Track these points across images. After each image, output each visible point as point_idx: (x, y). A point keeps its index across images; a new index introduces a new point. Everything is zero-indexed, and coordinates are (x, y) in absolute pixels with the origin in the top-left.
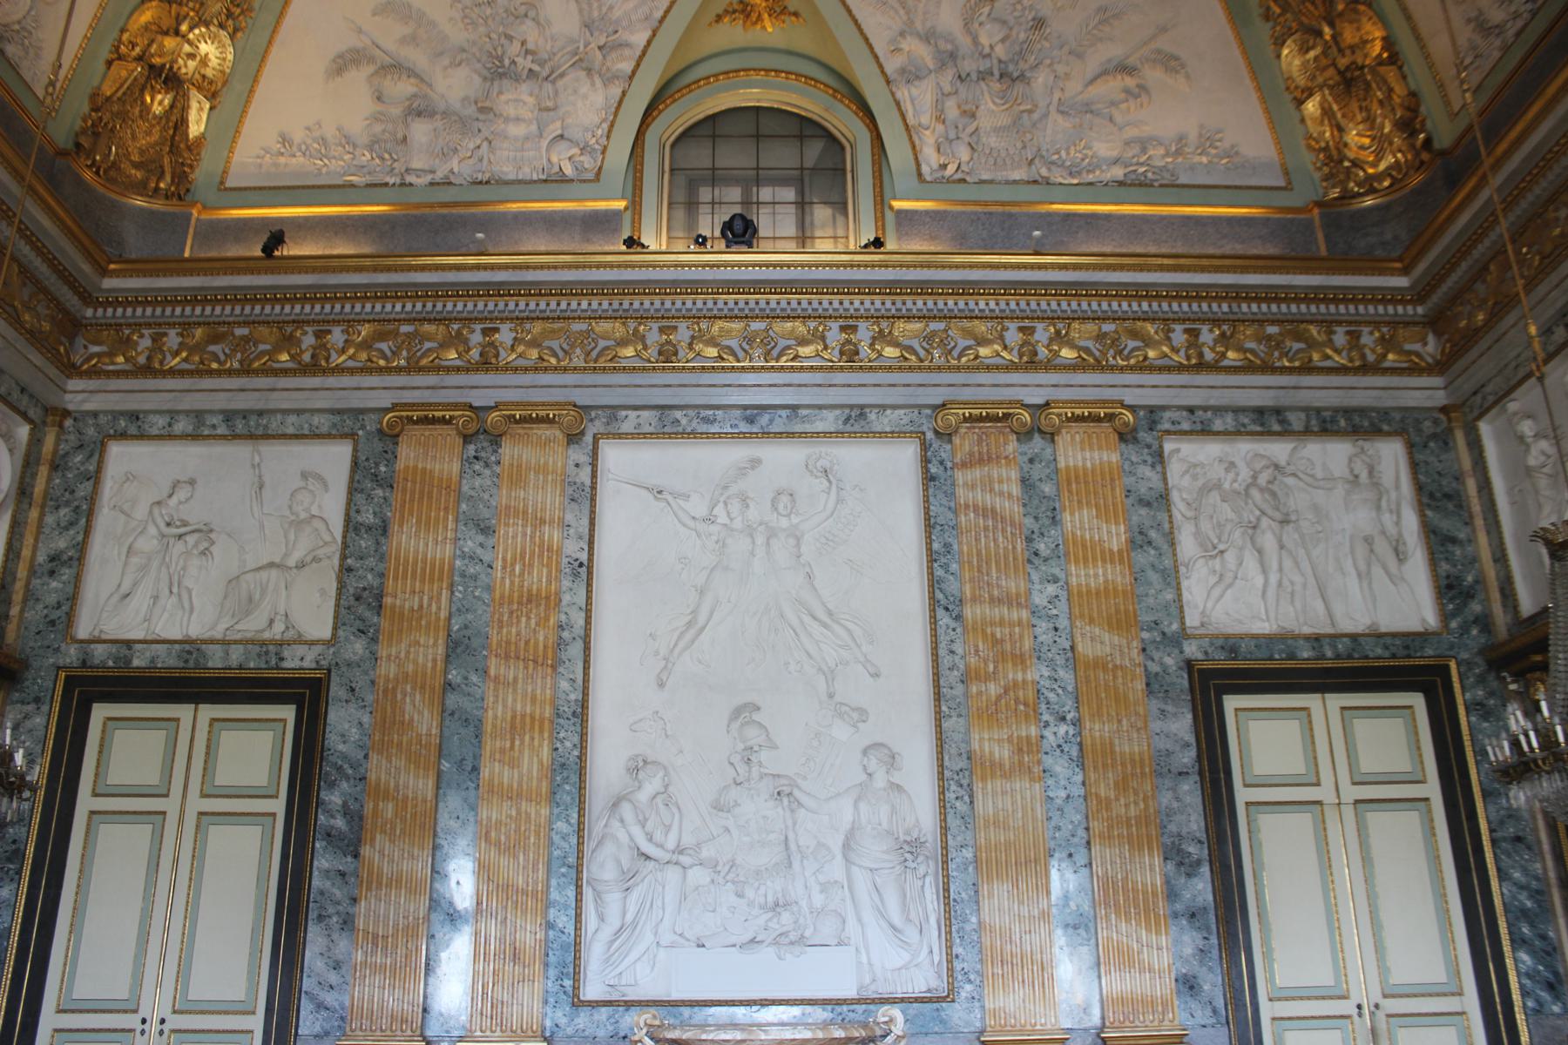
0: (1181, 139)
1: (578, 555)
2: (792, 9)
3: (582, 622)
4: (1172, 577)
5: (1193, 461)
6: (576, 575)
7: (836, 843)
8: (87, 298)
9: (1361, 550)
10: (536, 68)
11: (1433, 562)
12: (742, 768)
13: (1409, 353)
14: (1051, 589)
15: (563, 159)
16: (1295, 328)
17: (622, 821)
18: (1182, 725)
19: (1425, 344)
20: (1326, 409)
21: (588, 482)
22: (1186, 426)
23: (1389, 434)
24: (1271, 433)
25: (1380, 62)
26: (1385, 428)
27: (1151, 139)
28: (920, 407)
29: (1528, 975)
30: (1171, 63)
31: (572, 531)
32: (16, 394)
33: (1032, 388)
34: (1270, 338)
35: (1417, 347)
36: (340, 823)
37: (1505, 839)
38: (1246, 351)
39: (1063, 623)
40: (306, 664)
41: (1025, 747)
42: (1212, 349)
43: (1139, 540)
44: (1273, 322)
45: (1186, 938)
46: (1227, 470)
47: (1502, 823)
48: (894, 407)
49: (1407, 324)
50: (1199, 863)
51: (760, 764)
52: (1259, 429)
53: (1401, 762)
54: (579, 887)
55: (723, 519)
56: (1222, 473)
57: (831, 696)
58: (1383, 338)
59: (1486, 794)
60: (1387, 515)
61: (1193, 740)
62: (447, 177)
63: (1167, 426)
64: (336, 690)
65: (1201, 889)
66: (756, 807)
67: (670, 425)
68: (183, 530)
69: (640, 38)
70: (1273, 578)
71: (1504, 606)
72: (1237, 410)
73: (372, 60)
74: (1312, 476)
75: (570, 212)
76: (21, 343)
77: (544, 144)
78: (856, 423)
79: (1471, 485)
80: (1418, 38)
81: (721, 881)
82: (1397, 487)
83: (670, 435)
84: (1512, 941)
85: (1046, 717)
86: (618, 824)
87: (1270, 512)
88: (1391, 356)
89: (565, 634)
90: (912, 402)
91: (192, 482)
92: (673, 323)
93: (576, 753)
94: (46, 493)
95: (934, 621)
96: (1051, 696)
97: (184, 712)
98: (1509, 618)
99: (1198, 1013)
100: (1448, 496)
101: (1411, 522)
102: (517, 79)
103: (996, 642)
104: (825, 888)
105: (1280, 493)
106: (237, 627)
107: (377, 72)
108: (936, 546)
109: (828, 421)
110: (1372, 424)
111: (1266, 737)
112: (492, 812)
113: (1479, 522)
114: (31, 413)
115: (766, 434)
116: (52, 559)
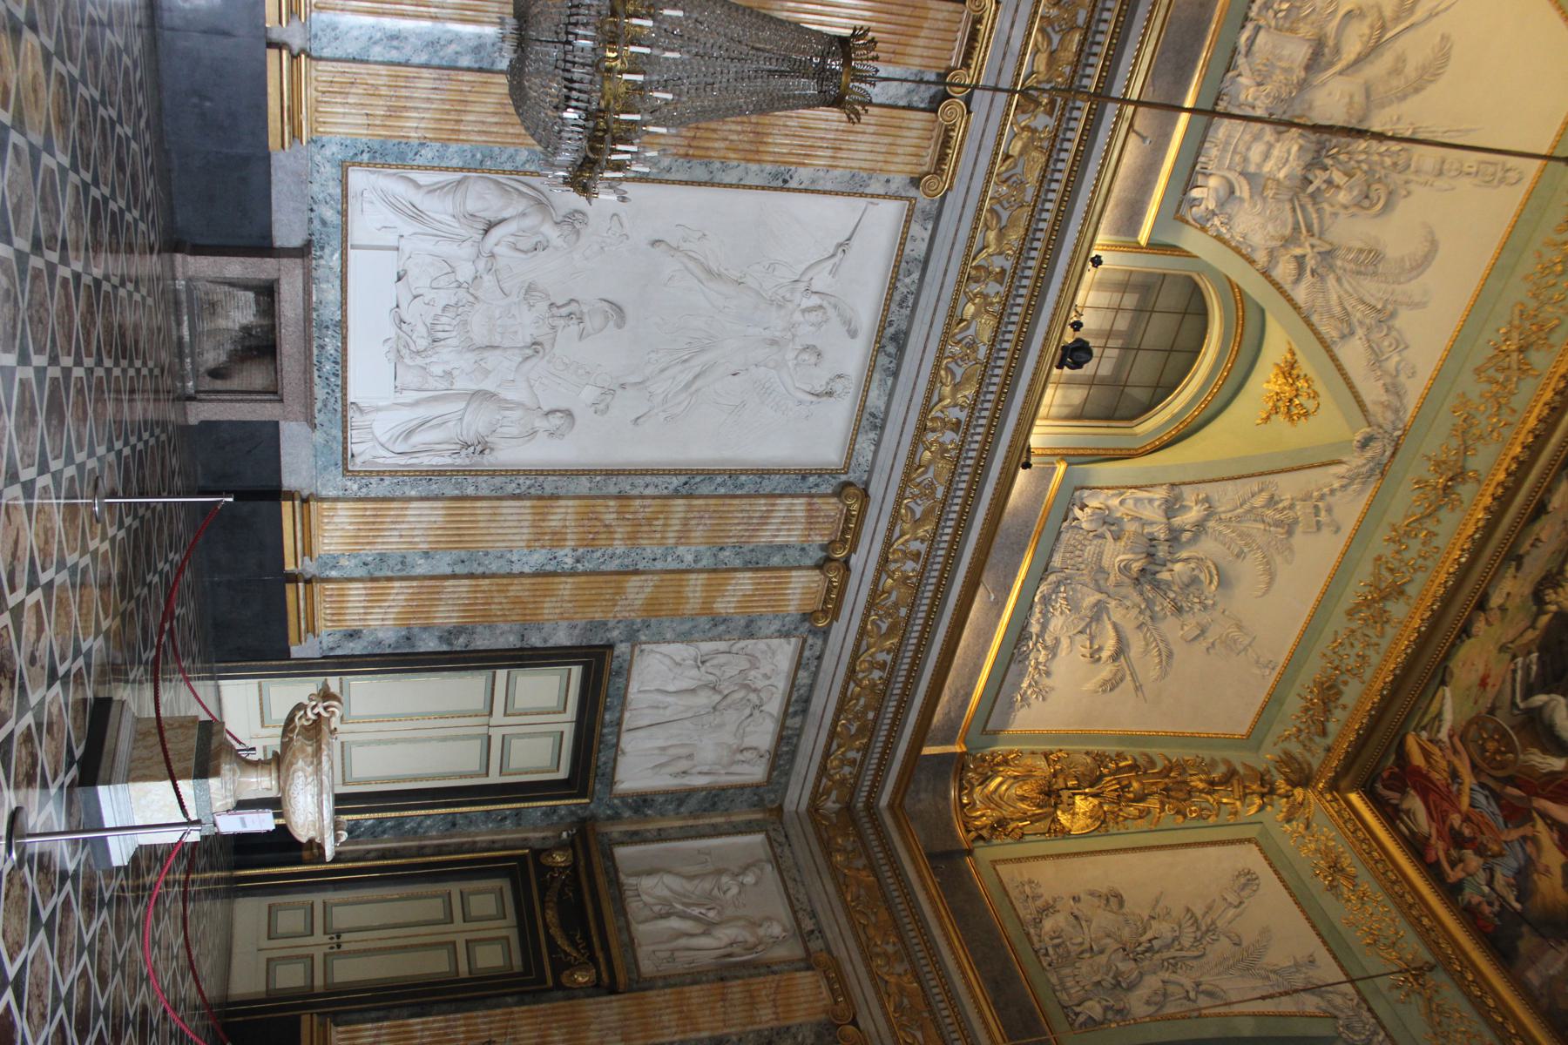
0: (1048, 674)
1: (796, 178)
2: (1273, 417)
3: (727, 180)
4: (685, 637)
5: (780, 656)
6: (776, 176)
7: (488, 385)
10: (1311, 189)
11: (666, 793)
12: (564, 311)
14: (689, 558)
15: (1206, 193)
16: (869, 730)
17: (524, 215)
18: (562, 638)
21: (868, 191)
22: (807, 653)
25: (1055, 820)
27: (1054, 655)
28: (870, 472)
30: (1112, 684)
31: (821, 174)
33: (864, 560)
34: (865, 713)
35: (834, 796)
39: (659, 565)
41: (558, 538)
43: (717, 620)
44: (875, 720)
45: (391, 633)
48: (875, 453)
49: (852, 794)
50: (450, 644)
54: (461, 169)
55: (806, 303)
56: (762, 671)
57: (623, 386)
61: (551, 643)
62: (1236, 67)
63: (810, 641)
65: (430, 644)
66: (527, 323)
67: (907, 269)
69: (1301, 294)
71: (626, 832)
72: (812, 687)
73: (1397, 19)
75: (1163, 158)
77: (1232, 176)
78: (869, 421)
80: (1059, 856)
83: (897, 266)
85: (581, 550)
86: (521, 209)
89: (717, 165)
90: (877, 470)
92: (1057, 112)
95: (677, 473)
96: (599, 554)
98: (615, 835)
99: (331, 639)
100: (714, 804)
102: (1309, 167)
103: (649, 521)
104: (448, 374)
107: (1381, 17)
108: (743, 478)
109: (876, 399)
111: (546, 692)
115: (879, 347)
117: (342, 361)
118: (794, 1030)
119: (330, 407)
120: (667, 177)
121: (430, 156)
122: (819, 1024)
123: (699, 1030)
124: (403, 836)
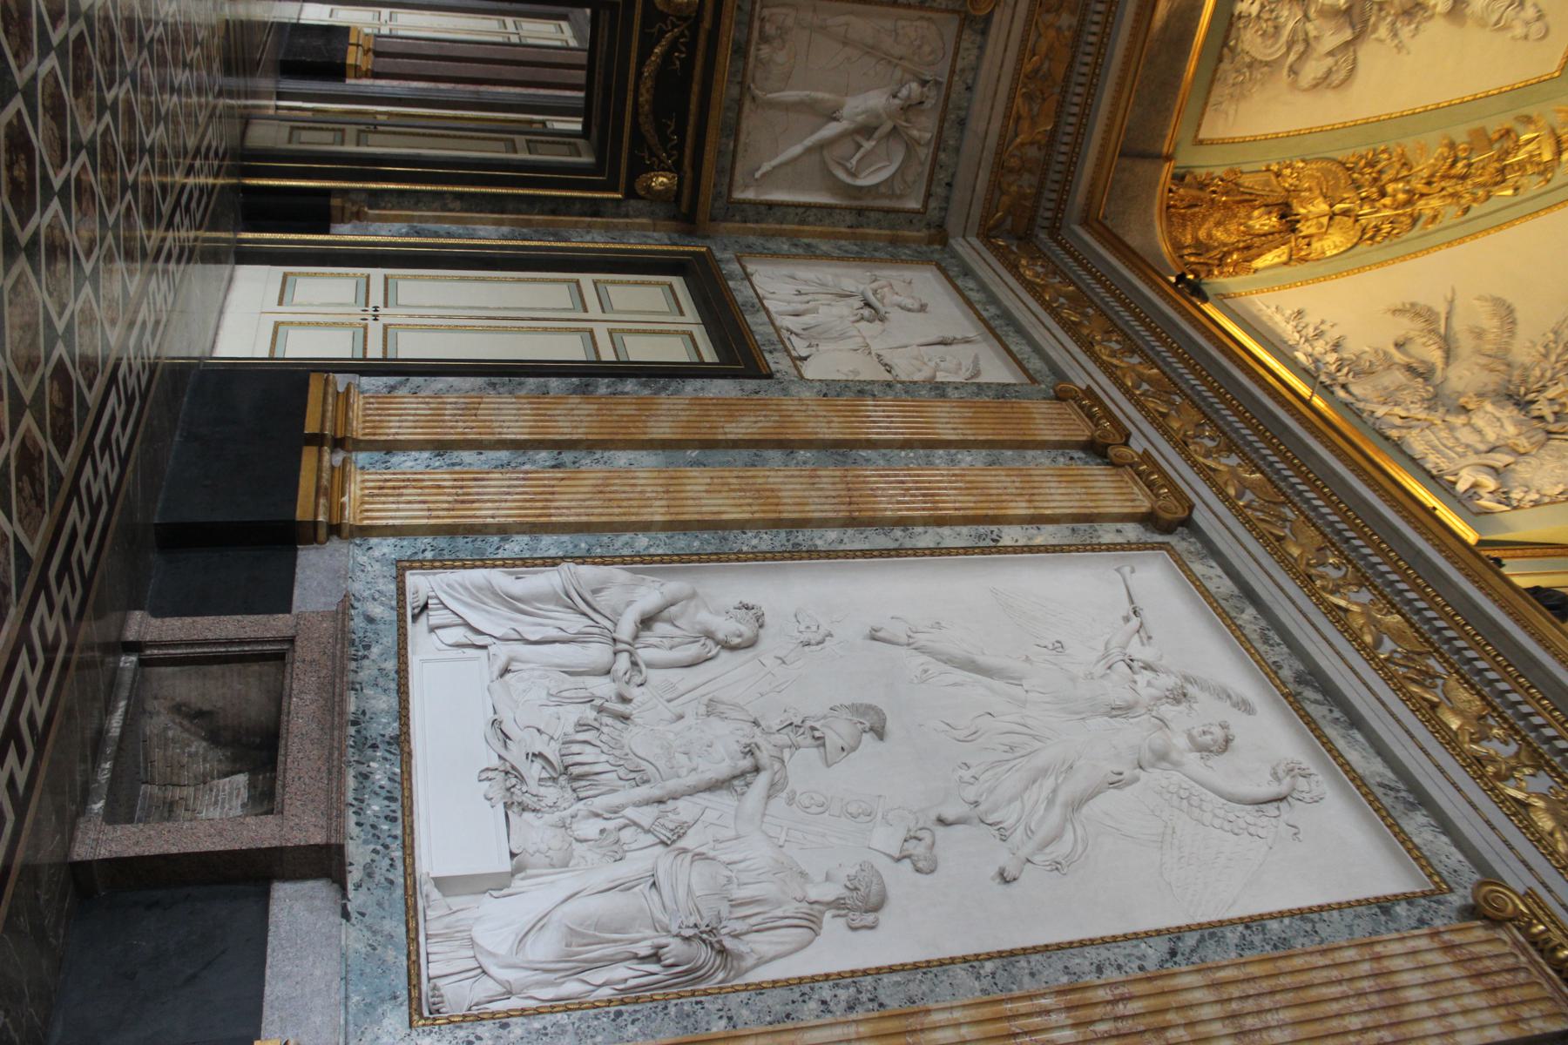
3: (921, 545)
8: (1054, 230)
32: (942, 176)
36: (603, 390)
40: (773, 367)
51: (795, 747)
64: (750, 384)
67: (1236, 608)
68: (873, 300)
76: (988, 156)
81: (597, 702)
91: (923, 308)
93: (745, 549)
94: (865, 237)
97: (691, 313)
106: (793, 338)
112: (643, 478)
114: (933, 204)
115: (1294, 700)
116: (809, 246)
117: (402, 796)
119: (377, 877)
120: (842, 547)
121: (517, 549)
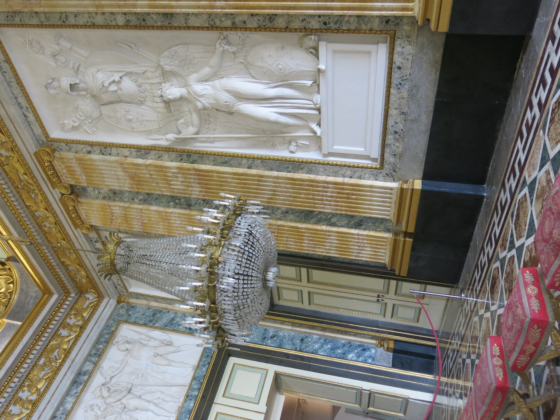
9: (159, 360)
13: (88, 307)
16: (45, 350)
19: (89, 298)
20: (91, 351)
23: (116, 329)
24: (87, 382)
26: (113, 329)
29: (358, 357)
34: (44, 364)
35: (88, 302)
37: (301, 346)
38: (42, 378)
42: (32, 394)
46: (92, 410)
47: (294, 344)
52: (81, 387)
53: (256, 377)
56: (93, 413)
58: (75, 314)
59: (280, 347)
60: (150, 342)
70: (152, 407)
72: (67, 393)
74: (117, 369)
79: (154, 304)
82: (141, 334)
84: (342, 359)
87: (120, 397)
88: (85, 315)
100: (154, 315)
101: (157, 334)
105: (116, 388)
110: (108, 334)
113: (169, 307)
118: (101, 196)
122: (86, 196)
123: (156, 211)
124: (333, 340)
